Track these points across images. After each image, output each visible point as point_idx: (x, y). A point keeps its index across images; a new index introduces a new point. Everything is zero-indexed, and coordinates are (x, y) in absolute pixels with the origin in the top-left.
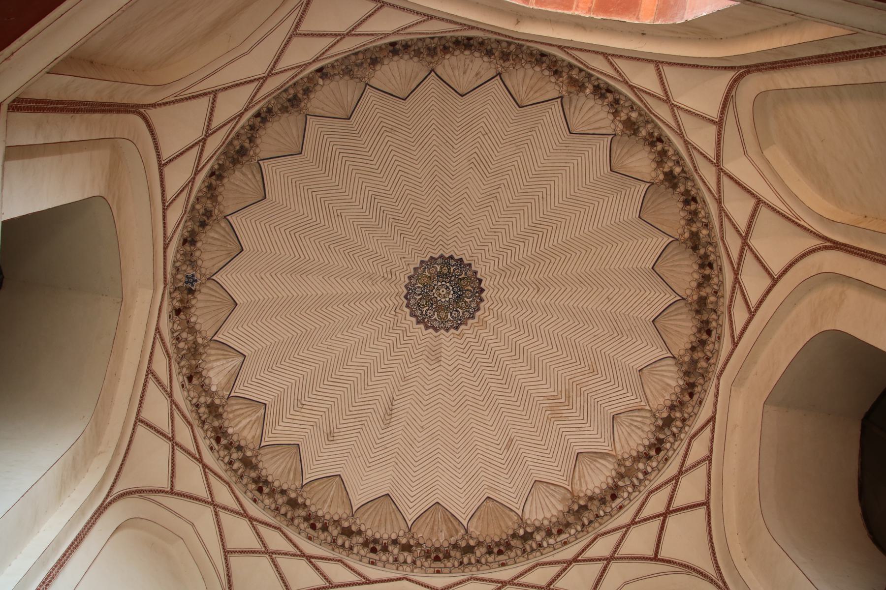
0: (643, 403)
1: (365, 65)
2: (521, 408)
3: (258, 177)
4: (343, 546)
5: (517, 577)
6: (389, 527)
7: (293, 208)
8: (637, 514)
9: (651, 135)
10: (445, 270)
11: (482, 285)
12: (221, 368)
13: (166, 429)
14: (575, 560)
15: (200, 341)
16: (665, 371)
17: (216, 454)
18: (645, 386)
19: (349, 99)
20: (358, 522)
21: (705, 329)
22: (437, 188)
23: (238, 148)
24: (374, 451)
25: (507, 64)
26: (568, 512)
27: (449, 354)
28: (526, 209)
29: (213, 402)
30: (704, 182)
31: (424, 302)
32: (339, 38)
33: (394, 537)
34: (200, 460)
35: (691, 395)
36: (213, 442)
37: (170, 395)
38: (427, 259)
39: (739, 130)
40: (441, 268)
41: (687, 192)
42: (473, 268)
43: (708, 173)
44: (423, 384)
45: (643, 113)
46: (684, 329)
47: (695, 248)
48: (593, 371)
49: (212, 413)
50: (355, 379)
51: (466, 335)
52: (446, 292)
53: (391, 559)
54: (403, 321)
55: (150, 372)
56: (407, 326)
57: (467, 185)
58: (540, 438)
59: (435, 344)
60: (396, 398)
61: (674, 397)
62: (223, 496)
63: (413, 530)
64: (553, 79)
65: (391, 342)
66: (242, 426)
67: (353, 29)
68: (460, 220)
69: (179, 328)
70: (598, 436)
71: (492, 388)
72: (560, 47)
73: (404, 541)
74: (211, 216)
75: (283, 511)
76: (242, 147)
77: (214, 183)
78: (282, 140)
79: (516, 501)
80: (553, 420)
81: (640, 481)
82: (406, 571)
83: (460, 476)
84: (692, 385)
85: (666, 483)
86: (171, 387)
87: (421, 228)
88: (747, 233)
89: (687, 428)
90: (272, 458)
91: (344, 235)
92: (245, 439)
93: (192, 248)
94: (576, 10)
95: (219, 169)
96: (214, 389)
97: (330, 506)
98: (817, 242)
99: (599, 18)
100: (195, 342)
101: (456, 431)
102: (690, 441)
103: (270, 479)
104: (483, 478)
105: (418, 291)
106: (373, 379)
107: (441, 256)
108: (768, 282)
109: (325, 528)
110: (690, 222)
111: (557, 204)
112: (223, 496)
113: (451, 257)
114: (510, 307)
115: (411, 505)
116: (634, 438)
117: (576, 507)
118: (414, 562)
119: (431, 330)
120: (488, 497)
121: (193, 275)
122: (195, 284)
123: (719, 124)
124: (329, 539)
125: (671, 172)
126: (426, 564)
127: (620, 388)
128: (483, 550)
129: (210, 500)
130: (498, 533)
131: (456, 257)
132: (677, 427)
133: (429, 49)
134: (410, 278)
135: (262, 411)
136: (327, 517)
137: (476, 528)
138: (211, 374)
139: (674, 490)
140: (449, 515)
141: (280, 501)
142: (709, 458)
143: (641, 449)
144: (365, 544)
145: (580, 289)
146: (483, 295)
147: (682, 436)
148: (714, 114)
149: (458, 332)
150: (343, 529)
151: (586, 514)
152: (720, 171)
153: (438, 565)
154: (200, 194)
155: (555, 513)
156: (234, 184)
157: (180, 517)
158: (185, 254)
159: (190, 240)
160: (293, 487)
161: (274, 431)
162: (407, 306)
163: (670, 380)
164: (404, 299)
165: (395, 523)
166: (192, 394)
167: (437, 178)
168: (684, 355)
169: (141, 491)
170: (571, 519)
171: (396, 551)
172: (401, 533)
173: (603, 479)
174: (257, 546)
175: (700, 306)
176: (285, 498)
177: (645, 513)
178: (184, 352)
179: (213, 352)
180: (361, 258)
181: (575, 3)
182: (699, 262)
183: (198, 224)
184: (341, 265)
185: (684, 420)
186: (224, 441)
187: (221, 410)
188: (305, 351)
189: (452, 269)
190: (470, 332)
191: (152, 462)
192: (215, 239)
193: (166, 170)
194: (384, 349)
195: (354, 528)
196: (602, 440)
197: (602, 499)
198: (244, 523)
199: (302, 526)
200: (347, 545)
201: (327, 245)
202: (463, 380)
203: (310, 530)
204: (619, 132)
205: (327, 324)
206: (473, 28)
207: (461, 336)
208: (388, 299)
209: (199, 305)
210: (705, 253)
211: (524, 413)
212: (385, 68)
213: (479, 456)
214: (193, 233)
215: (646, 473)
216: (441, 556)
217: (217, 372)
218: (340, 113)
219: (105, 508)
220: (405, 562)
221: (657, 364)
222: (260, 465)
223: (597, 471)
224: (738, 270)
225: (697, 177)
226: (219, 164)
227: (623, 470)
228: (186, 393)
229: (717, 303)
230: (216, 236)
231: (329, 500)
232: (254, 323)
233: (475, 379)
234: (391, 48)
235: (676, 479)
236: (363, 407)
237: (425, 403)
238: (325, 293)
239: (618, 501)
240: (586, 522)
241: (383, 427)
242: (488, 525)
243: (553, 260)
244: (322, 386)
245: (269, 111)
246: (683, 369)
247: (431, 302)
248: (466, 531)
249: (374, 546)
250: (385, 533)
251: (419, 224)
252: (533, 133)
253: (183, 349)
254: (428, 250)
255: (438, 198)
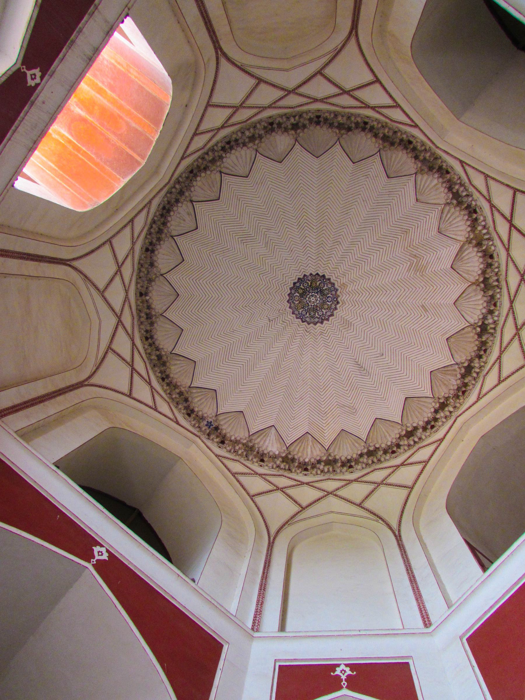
0: (440, 208)
1: (150, 270)
2: (407, 290)
3: (181, 358)
4: (415, 442)
5: (501, 347)
6: (426, 410)
7: (213, 352)
8: (504, 245)
9: (265, 128)
10: (301, 291)
11: (321, 275)
12: (271, 442)
13: (271, 487)
14: (512, 302)
15: (245, 441)
16: (425, 183)
17: (311, 475)
18: (429, 202)
19: (168, 289)
20: (408, 425)
21: (407, 144)
22: (249, 270)
23: (156, 358)
24: (378, 391)
25: (187, 194)
26: (485, 292)
27: (350, 315)
28: (286, 226)
29: (283, 458)
30: (301, 105)
31: (312, 313)
32: (119, 273)
33: (433, 410)
34: (302, 483)
35: (448, 172)
36: (305, 472)
37: (257, 474)
38: (288, 298)
39: (269, 69)
40: (298, 293)
41: (310, 120)
42: (308, 274)
43: (293, 100)
44: (358, 340)
45: (248, 127)
46: (401, 159)
47: (349, 129)
48: (406, 232)
49: (288, 461)
50: (331, 377)
51: (345, 300)
52: (313, 297)
53: (444, 420)
54: (316, 331)
55: (234, 474)
56: (320, 330)
57: (256, 252)
58: (432, 287)
59: (340, 320)
60: (357, 360)
61: (444, 185)
62: (330, 486)
63: (436, 396)
64: (208, 172)
65: (323, 345)
66: (310, 453)
67: (118, 263)
68: (275, 267)
69: (230, 447)
70: (448, 248)
71: (385, 301)
72: (183, 158)
73: (438, 405)
74: (183, 393)
75: (370, 462)
76: (157, 356)
77: (168, 381)
78: (170, 335)
79: (460, 323)
80: (424, 273)
81: (488, 233)
82: (454, 415)
83: (425, 350)
84: (440, 168)
85: (492, 215)
86: (253, 471)
87: (268, 291)
88: (341, 89)
89: (466, 185)
90: (339, 448)
91: (246, 335)
92: (317, 455)
93: (195, 413)
94: (154, 138)
95: (162, 374)
96: (277, 453)
97: (390, 435)
98: (353, 40)
99: (162, 127)
100: (243, 444)
101: (398, 337)
102: (472, 185)
103: (349, 457)
104: (435, 336)
105: (304, 313)
106: (338, 366)
107: (291, 289)
108: (377, 85)
109: (398, 446)
110: (331, 125)
111: (291, 206)
112: (330, 486)
113: (294, 284)
114: (342, 265)
115: (423, 389)
116: (460, 226)
117: (482, 285)
118: (455, 407)
119: (331, 318)
120: (447, 339)
121: (207, 422)
122: (212, 424)
123: (260, 81)
124: (406, 448)
125: (293, 125)
126: (461, 401)
127: (425, 219)
128: (477, 361)
129: (326, 493)
130: (473, 345)
131: (296, 281)
132: (462, 192)
133: (158, 232)
134: (293, 313)
135: (310, 436)
136: (394, 441)
137: (461, 357)
138: (269, 449)
139: (498, 211)
140: (443, 369)
141: (365, 461)
142: (486, 176)
143: (469, 223)
144: (424, 429)
145: (351, 216)
146: (327, 277)
147: (470, 190)
148: (253, 81)
149: (341, 303)
150: (405, 436)
151: (491, 281)
152: (293, 91)
153: (466, 394)
154: (168, 392)
155: (481, 302)
156: (177, 373)
157: (321, 515)
158: (194, 419)
159: (190, 412)
160: (363, 448)
161: (326, 438)
162: (309, 324)
163: (432, 183)
164: (304, 323)
165: (426, 404)
166: (270, 465)
167: (243, 267)
168: (417, 166)
169: (287, 522)
170: (490, 293)
171: (442, 414)
172: (433, 404)
173: (476, 259)
174: (372, 487)
175: (387, 141)
176: (366, 457)
177: (505, 239)
178: (245, 453)
179: (259, 440)
180: (265, 333)
181: (151, 138)
182: (360, 130)
183: (184, 403)
184: (262, 346)
185: (461, 185)
186: (309, 467)
187: (290, 456)
188: (297, 394)
189: (302, 287)
190: (344, 296)
191: (279, 508)
192: (200, 400)
193: (134, 395)
194: (324, 350)
195: (409, 429)
196: (452, 247)
197: (487, 266)
198: (355, 485)
199: (387, 458)
200: (416, 439)
201: (246, 347)
202: (369, 316)
203: (394, 455)
204: (255, 147)
205: (290, 373)
206: (150, 202)
207: (344, 303)
208: (298, 332)
209: (228, 431)
210: (355, 123)
211: (411, 289)
212: (160, 261)
213: (420, 331)
214: (186, 408)
215: (484, 227)
216: (464, 389)
217: (271, 446)
218: (173, 298)
219: (273, 542)
220: (451, 412)
221: (418, 187)
222: (337, 457)
223: (470, 260)
224: (366, 104)
225: (298, 109)
226: (159, 373)
227: (474, 242)
228: (266, 467)
229: (390, 129)
230: (199, 398)
231: (386, 434)
232: (262, 410)
233: (374, 309)
234: (149, 252)
235: (492, 206)
236: (350, 382)
237: (370, 345)
238: (272, 364)
239: (495, 255)
240: (496, 283)
241: (368, 377)
242: (464, 349)
243: (325, 224)
244: (322, 397)
245: (147, 331)
246: (426, 170)
247: (315, 309)
248: (457, 364)
249: (430, 425)
250: (428, 414)
251: (265, 291)
252: (241, 199)
253: (242, 452)
254: (283, 294)
255: (255, 273)
